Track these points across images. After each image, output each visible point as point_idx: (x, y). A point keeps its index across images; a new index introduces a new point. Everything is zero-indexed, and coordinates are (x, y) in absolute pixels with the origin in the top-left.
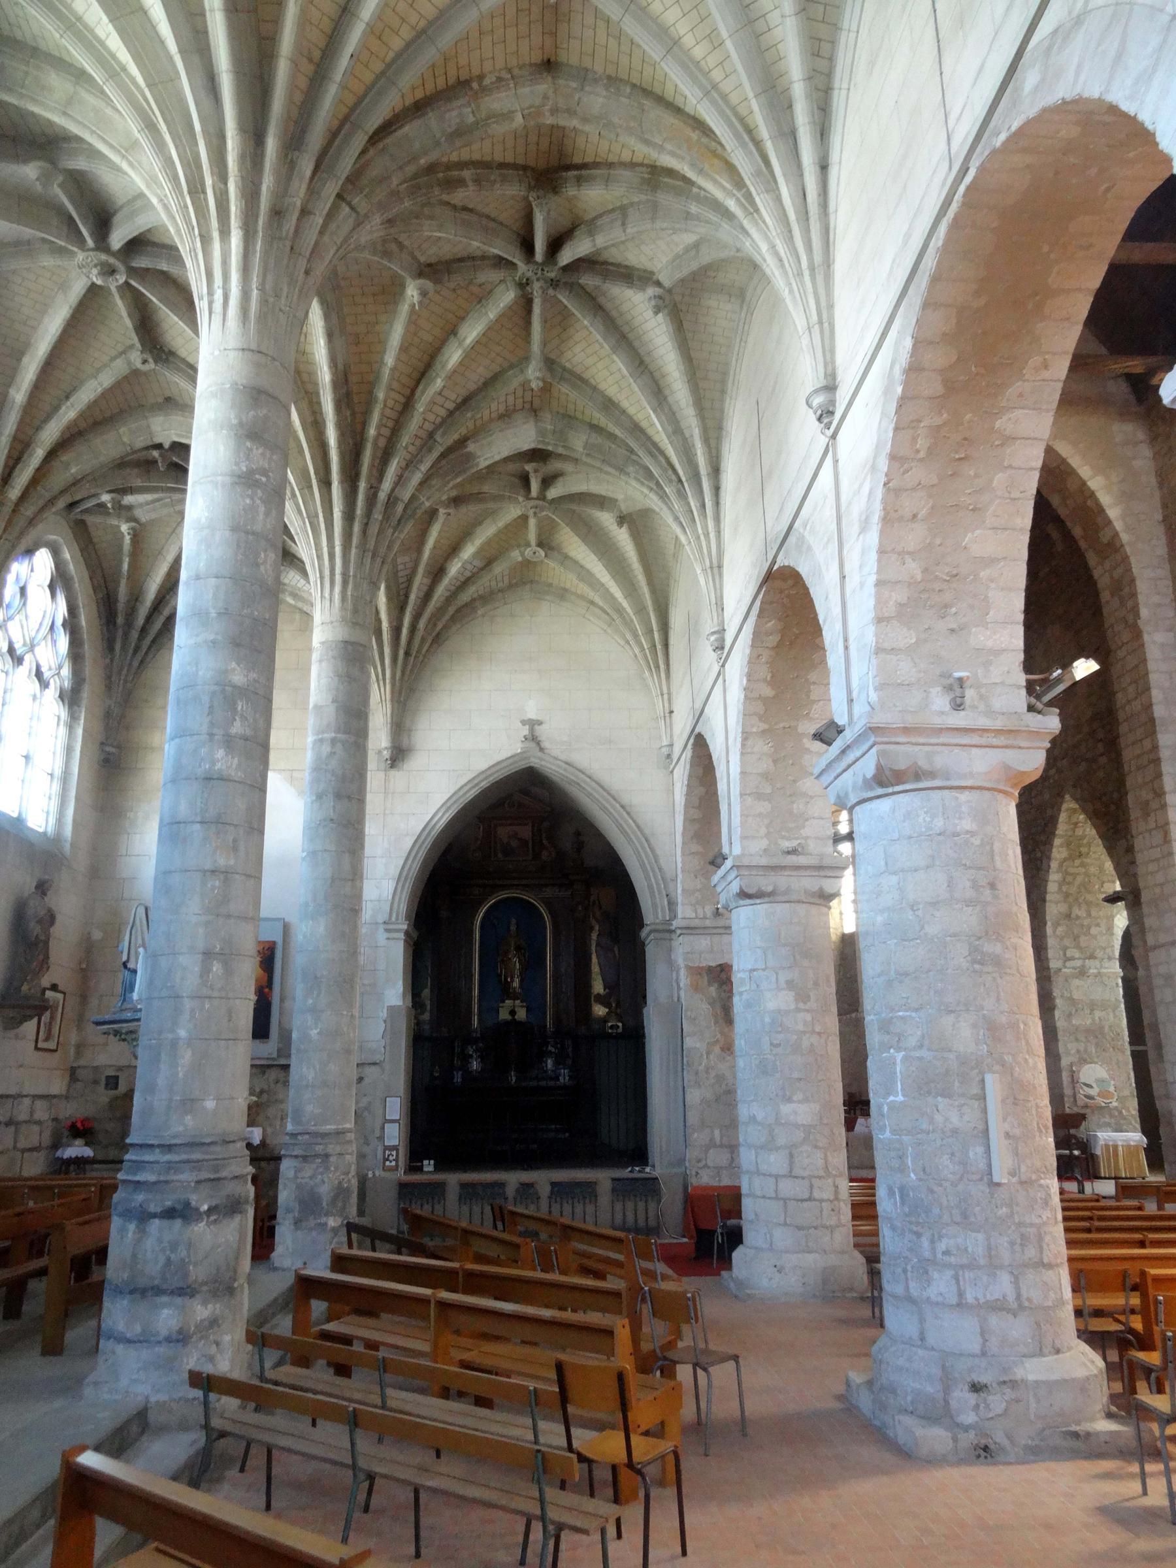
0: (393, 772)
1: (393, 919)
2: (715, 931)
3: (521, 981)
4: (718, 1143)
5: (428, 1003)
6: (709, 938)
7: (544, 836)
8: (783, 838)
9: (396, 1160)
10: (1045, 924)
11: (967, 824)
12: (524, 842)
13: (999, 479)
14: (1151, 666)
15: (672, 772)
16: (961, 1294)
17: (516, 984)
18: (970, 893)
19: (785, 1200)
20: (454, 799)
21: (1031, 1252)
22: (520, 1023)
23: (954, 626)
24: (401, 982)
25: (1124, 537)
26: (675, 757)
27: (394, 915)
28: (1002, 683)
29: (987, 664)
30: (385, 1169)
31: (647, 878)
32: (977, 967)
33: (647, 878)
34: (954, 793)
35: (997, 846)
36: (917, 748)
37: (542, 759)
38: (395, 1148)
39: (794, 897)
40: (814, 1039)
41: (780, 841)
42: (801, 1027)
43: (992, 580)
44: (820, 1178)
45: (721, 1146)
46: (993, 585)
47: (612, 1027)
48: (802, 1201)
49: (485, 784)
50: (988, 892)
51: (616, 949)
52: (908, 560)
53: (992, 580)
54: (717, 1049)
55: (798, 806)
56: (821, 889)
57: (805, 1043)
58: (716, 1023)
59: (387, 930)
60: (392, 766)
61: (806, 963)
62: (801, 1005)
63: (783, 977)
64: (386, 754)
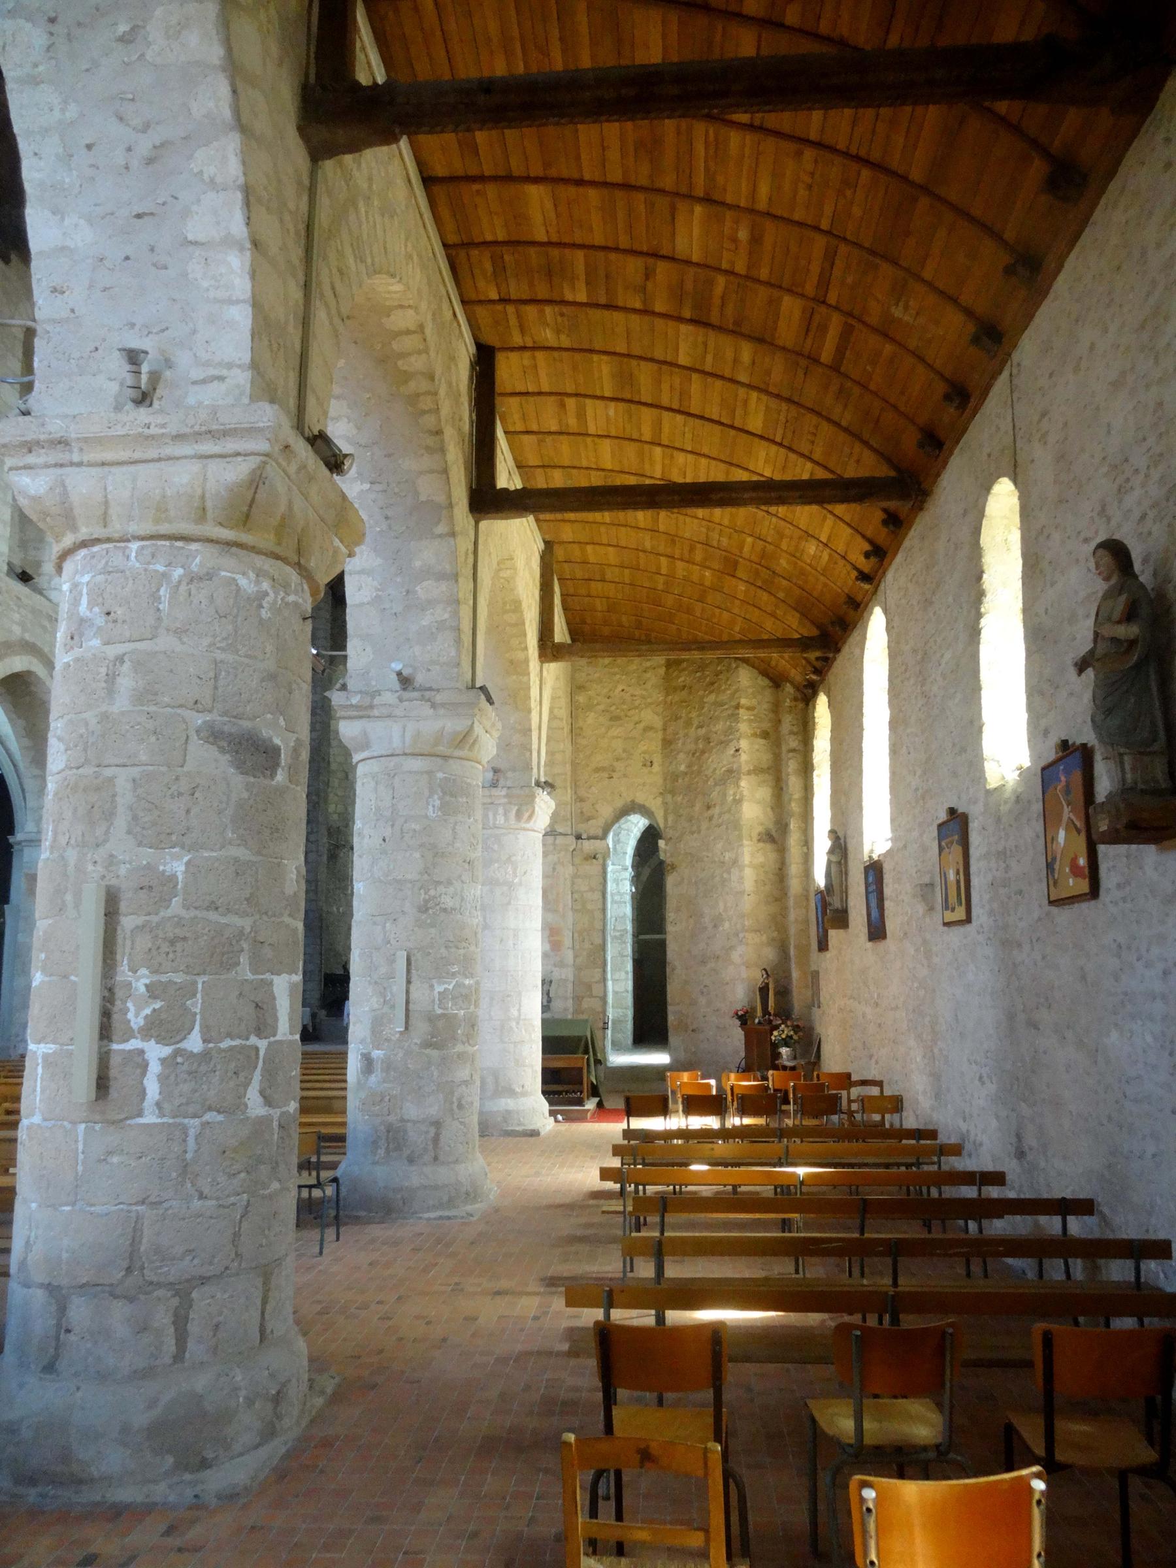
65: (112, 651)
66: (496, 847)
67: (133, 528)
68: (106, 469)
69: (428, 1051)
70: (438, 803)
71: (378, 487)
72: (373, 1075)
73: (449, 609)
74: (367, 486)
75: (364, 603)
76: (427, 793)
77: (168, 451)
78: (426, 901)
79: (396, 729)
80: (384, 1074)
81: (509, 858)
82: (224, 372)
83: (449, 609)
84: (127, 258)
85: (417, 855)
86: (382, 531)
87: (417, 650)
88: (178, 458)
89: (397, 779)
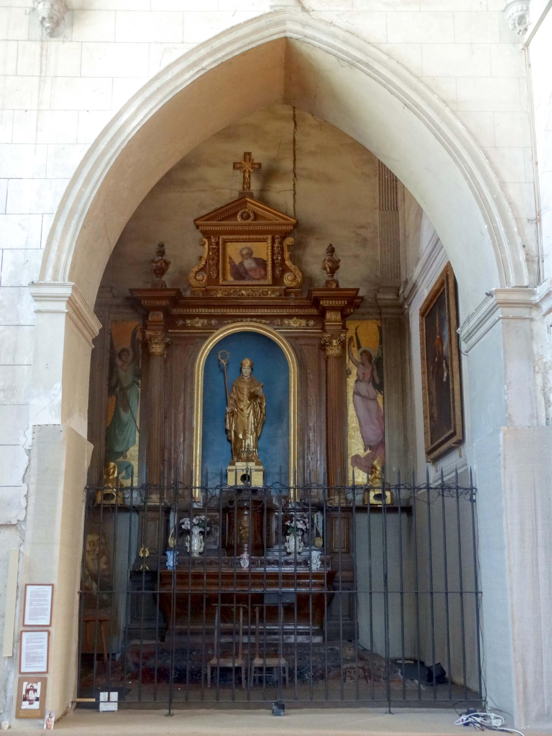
0: (53, 44)
1: (48, 279)
3: (258, 438)
5: (135, 464)
7: (287, 255)
12: (261, 263)
15: (527, 45)
17: (250, 441)
20: (157, 84)
22: (255, 491)
24: (59, 385)
26: (533, 18)
27: (50, 271)
31: (489, 218)
33: (489, 218)
37: (304, 25)
38: (41, 678)
47: (377, 497)
49: (209, 64)
51: (380, 400)
59: (37, 298)
60: (53, 33)
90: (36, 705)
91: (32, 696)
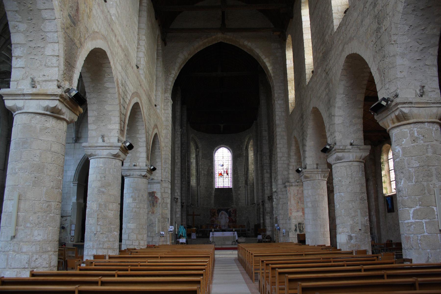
2: (152, 183)
4: (149, 236)
6: (150, 185)
8: (134, 162)
9: (74, 239)
10: (272, 178)
11: (101, 165)
13: (109, 95)
14: (276, 110)
16: (88, 253)
18: (99, 179)
19: (127, 245)
21: (101, 246)
23: (104, 125)
24: (76, 196)
25: (272, 75)
28: (113, 136)
29: (111, 132)
30: (71, 241)
32: (99, 193)
34: (100, 159)
35: (107, 169)
36: (93, 150)
39: (135, 176)
40: (137, 209)
41: (133, 163)
42: (133, 206)
43: (111, 115)
44: (135, 240)
45: (150, 236)
46: (112, 116)
48: (130, 245)
50: (103, 178)
52: (94, 111)
53: (111, 115)
54: (150, 213)
55: (138, 155)
56: (141, 174)
57: (134, 210)
58: (151, 206)
59: (73, 183)
61: (136, 192)
62: (134, 202)
63: (130, 195)
64: (74, 139)
65: (426, 144)
66: (319, 185)
67: (426, 120)
68: (419, 108)
69: (365, 234)
70: (361, 173)
71: (347, 96)
72: (353, 240)
73: (360, 126)
74: (344, 96)
75: (339, 124)
76: (359, 171)
77: (431, 105)
78: (361, 197)
79: (351, 155)
80: (356, 240)
81: (322, 188)
82: (435, 90)
83: (360, 126)
84: (415, 67)
85: (358, 186)
86: (346, 106)
87: (353, 135)
88: (433, 107)
89: (352, 168)
90: (73, 240)
91: (72, 239)
